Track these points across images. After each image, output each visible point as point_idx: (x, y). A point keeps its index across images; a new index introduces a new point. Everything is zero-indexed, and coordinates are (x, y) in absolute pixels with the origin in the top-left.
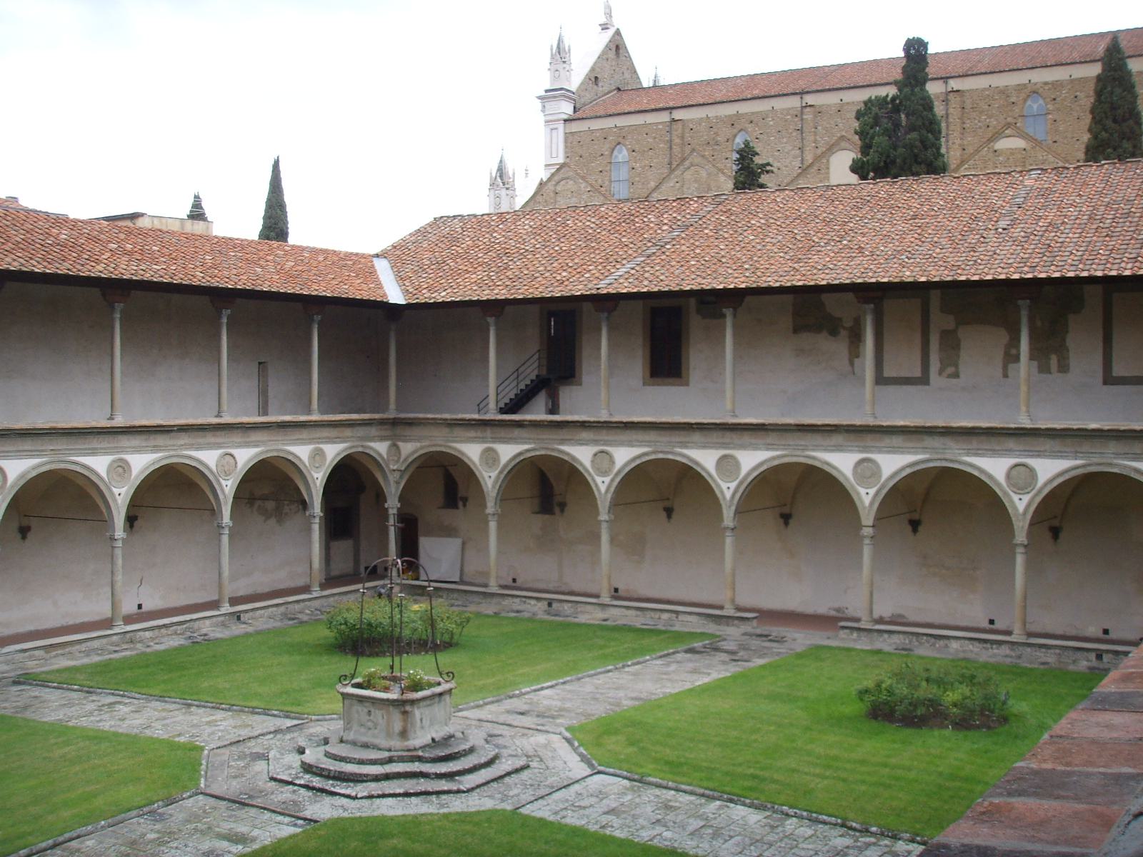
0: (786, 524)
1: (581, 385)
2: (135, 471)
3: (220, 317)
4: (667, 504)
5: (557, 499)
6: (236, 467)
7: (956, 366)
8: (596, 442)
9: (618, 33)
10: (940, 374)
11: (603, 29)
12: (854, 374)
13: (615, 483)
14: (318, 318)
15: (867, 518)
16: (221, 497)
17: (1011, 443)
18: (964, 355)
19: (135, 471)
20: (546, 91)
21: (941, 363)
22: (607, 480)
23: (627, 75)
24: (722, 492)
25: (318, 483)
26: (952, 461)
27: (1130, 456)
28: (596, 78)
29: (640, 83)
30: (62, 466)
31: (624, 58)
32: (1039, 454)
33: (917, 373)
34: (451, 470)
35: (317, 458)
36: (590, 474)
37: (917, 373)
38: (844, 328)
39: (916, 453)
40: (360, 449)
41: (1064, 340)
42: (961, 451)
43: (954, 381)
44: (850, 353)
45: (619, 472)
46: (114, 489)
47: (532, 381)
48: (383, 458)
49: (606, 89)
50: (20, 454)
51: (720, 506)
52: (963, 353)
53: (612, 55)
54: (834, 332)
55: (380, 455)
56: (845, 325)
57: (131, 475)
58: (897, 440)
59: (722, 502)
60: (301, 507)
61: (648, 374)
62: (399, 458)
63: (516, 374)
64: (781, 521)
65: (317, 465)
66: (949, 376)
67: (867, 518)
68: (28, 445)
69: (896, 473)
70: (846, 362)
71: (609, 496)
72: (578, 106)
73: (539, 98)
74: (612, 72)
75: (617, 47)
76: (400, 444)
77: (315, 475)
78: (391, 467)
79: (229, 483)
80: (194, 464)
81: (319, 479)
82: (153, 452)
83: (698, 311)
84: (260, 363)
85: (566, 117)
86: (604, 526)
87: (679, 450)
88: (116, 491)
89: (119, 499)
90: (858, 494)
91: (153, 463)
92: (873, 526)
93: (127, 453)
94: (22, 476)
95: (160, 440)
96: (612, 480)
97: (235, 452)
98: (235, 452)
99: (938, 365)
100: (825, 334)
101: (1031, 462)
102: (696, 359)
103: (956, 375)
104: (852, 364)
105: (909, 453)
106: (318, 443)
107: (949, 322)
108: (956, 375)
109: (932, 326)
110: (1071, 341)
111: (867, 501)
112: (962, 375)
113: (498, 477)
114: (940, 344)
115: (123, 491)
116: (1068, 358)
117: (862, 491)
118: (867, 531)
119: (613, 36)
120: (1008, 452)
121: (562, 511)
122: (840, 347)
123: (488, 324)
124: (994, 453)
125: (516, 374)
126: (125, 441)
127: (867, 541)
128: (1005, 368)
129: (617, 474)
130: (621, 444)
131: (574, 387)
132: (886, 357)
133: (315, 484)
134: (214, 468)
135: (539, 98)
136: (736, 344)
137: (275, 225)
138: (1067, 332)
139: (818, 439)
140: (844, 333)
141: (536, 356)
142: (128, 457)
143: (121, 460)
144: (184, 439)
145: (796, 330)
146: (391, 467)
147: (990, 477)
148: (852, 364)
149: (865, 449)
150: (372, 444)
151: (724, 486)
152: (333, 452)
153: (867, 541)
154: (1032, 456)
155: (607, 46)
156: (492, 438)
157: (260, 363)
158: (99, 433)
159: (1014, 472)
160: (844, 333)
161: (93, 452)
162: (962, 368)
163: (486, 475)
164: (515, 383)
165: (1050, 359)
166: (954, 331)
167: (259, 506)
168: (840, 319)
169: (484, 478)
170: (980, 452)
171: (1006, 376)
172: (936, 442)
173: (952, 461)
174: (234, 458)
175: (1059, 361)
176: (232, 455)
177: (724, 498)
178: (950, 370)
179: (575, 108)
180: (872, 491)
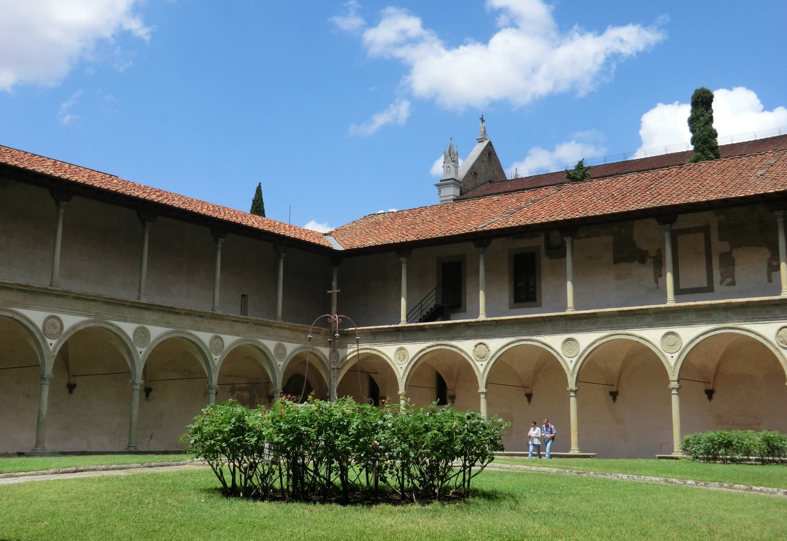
0: (614, 399)
1: (466, 312)
2: (153, 337)
3: (217, 243)
4: (528, 391)
5: (449, 393)
6: (223, 347)
7: (733, 276)
9: (490, 144)
10: (722, 282)
11: (479, 142)
12: (658, 288)
13: (490, 365)
14: (283, 255)
15: (673, 375)
16: (212, 366)
18: (738, 270)
19: (153, 337)
20: (441, 181)
21: (721, 276)
22: (485, 363)
23: (496, 173)
24: (566, 364)
25: (280, 368)
28: (475, 173)
29: (506, 178)
30: (102, 325)
31: (494, 161)
33: (705, 284)
34: (373, 376)
35: (280, 351)
37: (705, 284)
38: (650, 257)
40: (311, 350)
43: (732, 288)
44: (655, 276)
45: (493, 356)
46: (138, 348)
47: (431, 309)
48: (326, 359)
49: (482, 181)
50: (73, 312)
51: (565, 375)
52: (736, 266)
53: (485, 158)
54: (643, 261)
55: (324, 356)
56: (650, 255)
57: (150, 340)
59: (567, 372)
60: (267, 400)
61: (512, 301)
62: (338, 361)
63: (420, 305)
64: (611, 398)
65: (281, 356)
66: (729, 285)
67: (673, 375)
68: (80, 305)
70: (653, 281)
71: (486, 374)
72: (463, 191)
73: (437, 185)
74: (487, 170)
75: (490, 154)
76: (339, 350)
77: (279, 363)
78: (332, 366)
79: (218, 357)
80: (194, 340)
81: (281, 366)
82: (165, 326)
83: (547, 255)
84: (243, 296)
85: (455, 198)
86: (483, 396)
87: (534, 338)
88: (139, 349)
89: (141, 356)
91: (166, 335)
92: (678, 381)
93: (148, 324)
94: (73, 328)
95: (171, 318)
96: (488, 363)
97: (223, 336)
98: (223, 336)
99: (720, 277)
100: (636, 262)
102: (546, 288)
103: (733, 283)
104: (657, 282)
106: (281, 341)
107: (725, 247)
108: (733, 283)
109: (713, 252)
111: (672, 362)
112: (737, 283)
113: (407, 368)
114: (720, 262)
115: (144, 350)
117: (669, 356)
118: (674, 384)
119: (487, 146)
120: (775, 318)
121: (453, 402)
122: (647, 272)
123: (401, 263)
125: (420, 305)
126: (146, 314)
127: (674, 392)
128: (769, 276)
129: (491, 359)
130: (494, 337)
131: (462, 314)
132: (681, 274)
133: (278, 369)
134: (208, 345)
135: (437, 185)
136: (575, 264)
137: (258, 208)
140: (650, 261)
141: (435, 291)
142: (149, 327)
143: (145, 328)
144: (187, 321)
145: (616, 262)
146: (332, 366)
148: (657, 282)
150: (319, 348)
152: (291, 348)
153: (674, 392)
155: (482, 152)
157: (243, 296)
158: (131, 306)
159: (781, 332)
160: (650, 261)
161: (125, 320)
162: (737, 278)
163: (398, 367)
164: (419, 312)
166: (730, 252)
167: (238, 395)
168: (647, 252)
171: (770, 281)
174: (222, 340)
176: (221, 339)
177: (568, 369)
178: (729, 280)
179: (461, 192)
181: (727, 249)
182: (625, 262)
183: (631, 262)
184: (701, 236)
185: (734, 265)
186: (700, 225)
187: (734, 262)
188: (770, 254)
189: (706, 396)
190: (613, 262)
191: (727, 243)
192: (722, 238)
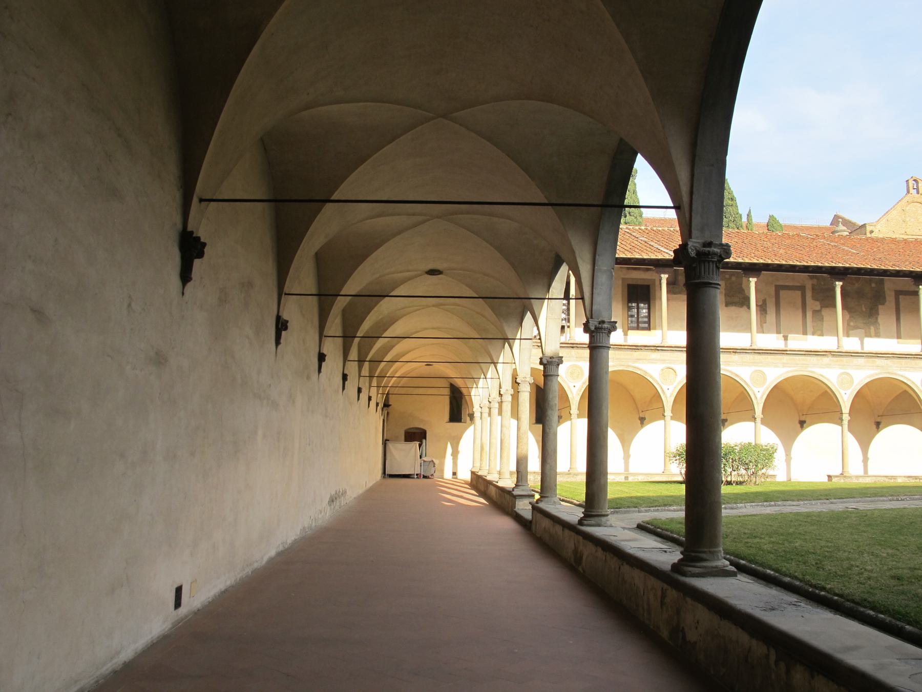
4: (642, 415)
8: (663, 361)
21: (814, 329)
36: (658, 383)
41: (877, 318)
44: (761, 321)
52: (825, 323)
90: (840, 394)
107: (817, 305)
109: (807, 307)
117: (842, 392)
138: (878, 314)
139: (813, 359)
147: (913, 383)
151: (756, 390)
156: (577, 358)
165: (870, 329)
166: (820, 311)
169: (569, 387)
170: (907, 369)
175: (875, 330)
180: (848, 392)
181: (818, 308)
182: (735, 306)
183: (741, 307)
184: (799, 293)
185: (823, 321)
186: (798, 284)
187: (823, 319)
188: (849, 316)
189: (799, 425)
190: (724, 305)
191: (818, 303)
192: (815, 298)
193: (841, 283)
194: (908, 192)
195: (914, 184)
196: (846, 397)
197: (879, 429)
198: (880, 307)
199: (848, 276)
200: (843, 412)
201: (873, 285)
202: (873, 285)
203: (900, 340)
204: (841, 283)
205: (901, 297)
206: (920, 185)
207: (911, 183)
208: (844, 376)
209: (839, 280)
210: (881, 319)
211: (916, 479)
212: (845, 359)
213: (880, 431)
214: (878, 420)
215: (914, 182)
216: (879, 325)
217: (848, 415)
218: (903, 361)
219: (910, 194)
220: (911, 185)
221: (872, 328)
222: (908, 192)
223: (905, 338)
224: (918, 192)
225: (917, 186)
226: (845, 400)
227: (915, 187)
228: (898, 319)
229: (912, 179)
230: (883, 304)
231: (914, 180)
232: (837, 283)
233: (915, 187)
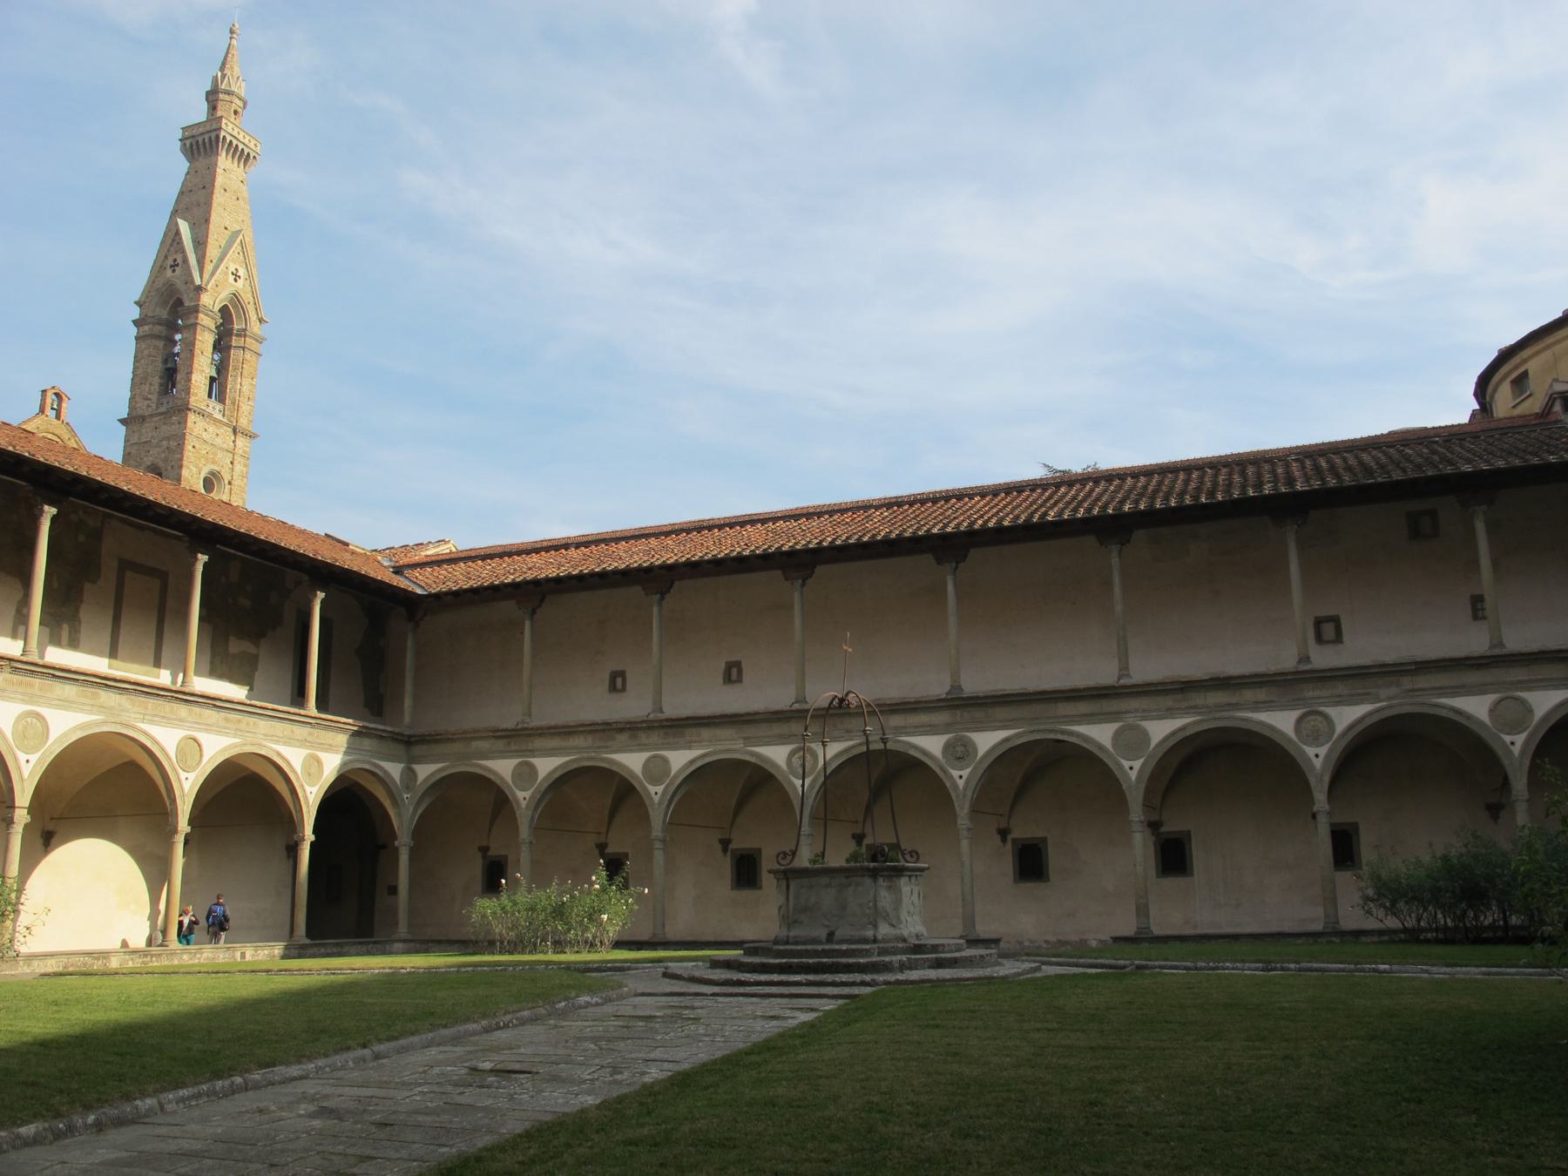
17: (183, 710)
26: (128, 726)
27: (275, 738)
32: (208, 728)
39: (91, 713)
41: (77, 610)
42: (138, 716)
58: (69, 690)
67: (23, 797)
69: (65, 735)
90: (16, 759)
101: (198, 735)
105: (82, 711)
110: (81, 615)
116: (80, 632)
117: (22, 757)
120: (180, 722)
124: (168, 721)
138: (82, 601)
147: (163, 750)
149: (30, 699)
154: (201, 730)
170: (156, 719)
172: (109, 698)
173: (128, 726)
175: (70, 632)
180: (34, 758)
193: (54, 511)
194: (42, 410)
195: (53, 400)
196: (26, 770)
197: (49, 848)
198: (87, 586)
199: (71, 499)
200: (17, 805)
201: (82, 538)
202: (82, 538)
203: (114, 662)
204: (54, 511)
205: (128, 574)
206: (64, 405)
207: (50, 397)
208: (29, 719)
209: (51, 504)
210: (85, 614)
211: (146, 956)
212: (37, 681)
213: (53, 850)
214: (50, 827)
215: (54, 397)
216: (80, 623)
217: (26, 811)
218: (152, 703)
219: (43, 416)
220: (49, 401)
221: (66, 627)
222: (42, 410)
223: (124, 660)
224: (58, 417)
225: (60, 405)
226: (26, 775)
227: (55, 407)
228: (117, 620)
229: (54, 391)
230: (94, 582)
231: (56, 394)
232: (46, 508)
233: (55, 407)
